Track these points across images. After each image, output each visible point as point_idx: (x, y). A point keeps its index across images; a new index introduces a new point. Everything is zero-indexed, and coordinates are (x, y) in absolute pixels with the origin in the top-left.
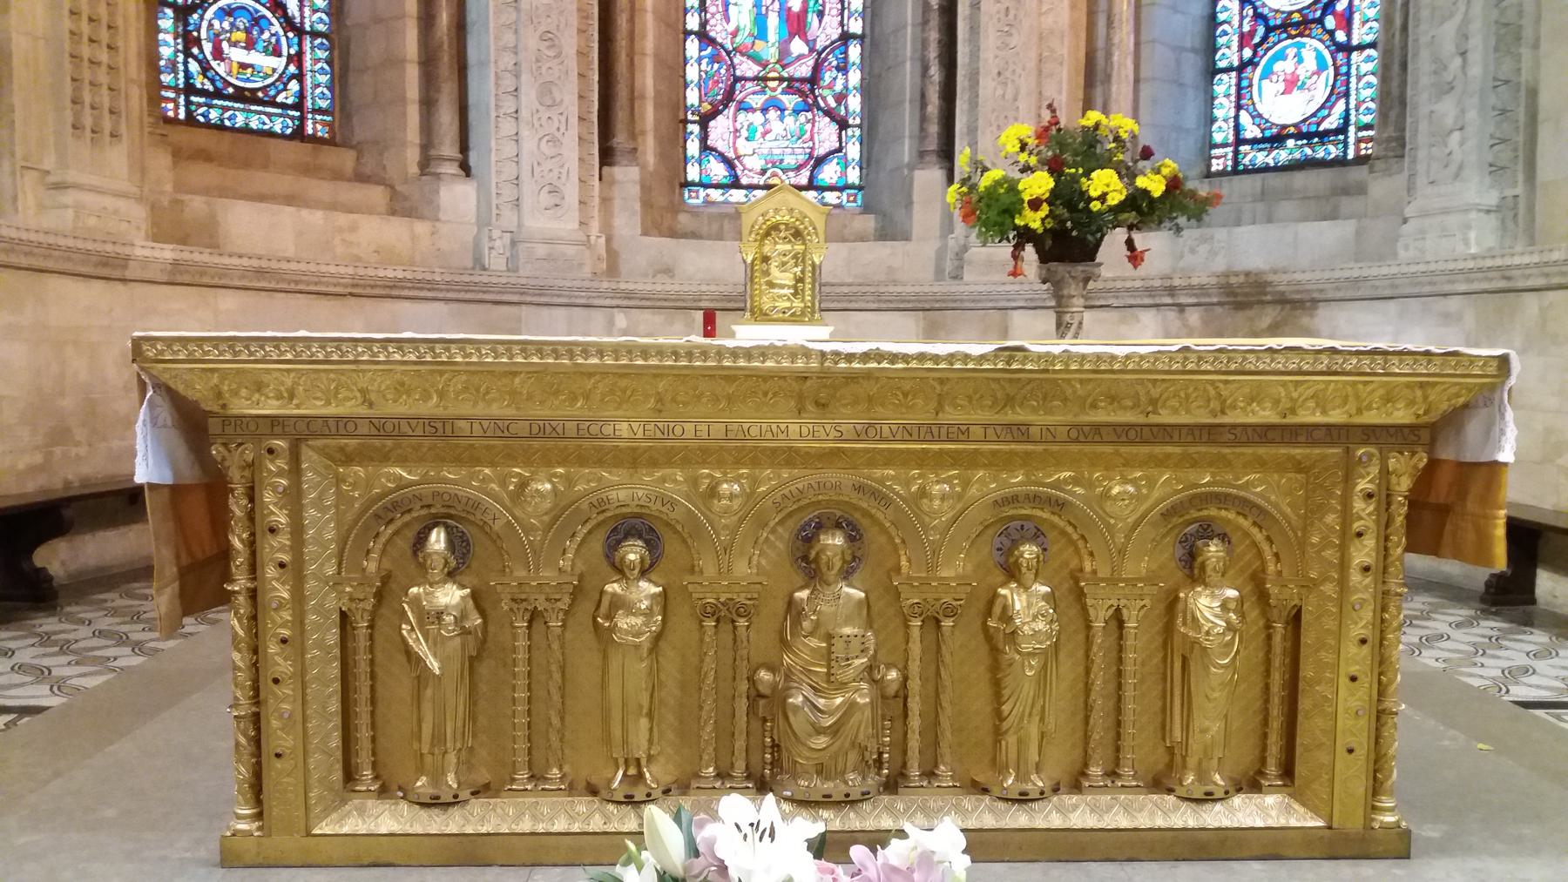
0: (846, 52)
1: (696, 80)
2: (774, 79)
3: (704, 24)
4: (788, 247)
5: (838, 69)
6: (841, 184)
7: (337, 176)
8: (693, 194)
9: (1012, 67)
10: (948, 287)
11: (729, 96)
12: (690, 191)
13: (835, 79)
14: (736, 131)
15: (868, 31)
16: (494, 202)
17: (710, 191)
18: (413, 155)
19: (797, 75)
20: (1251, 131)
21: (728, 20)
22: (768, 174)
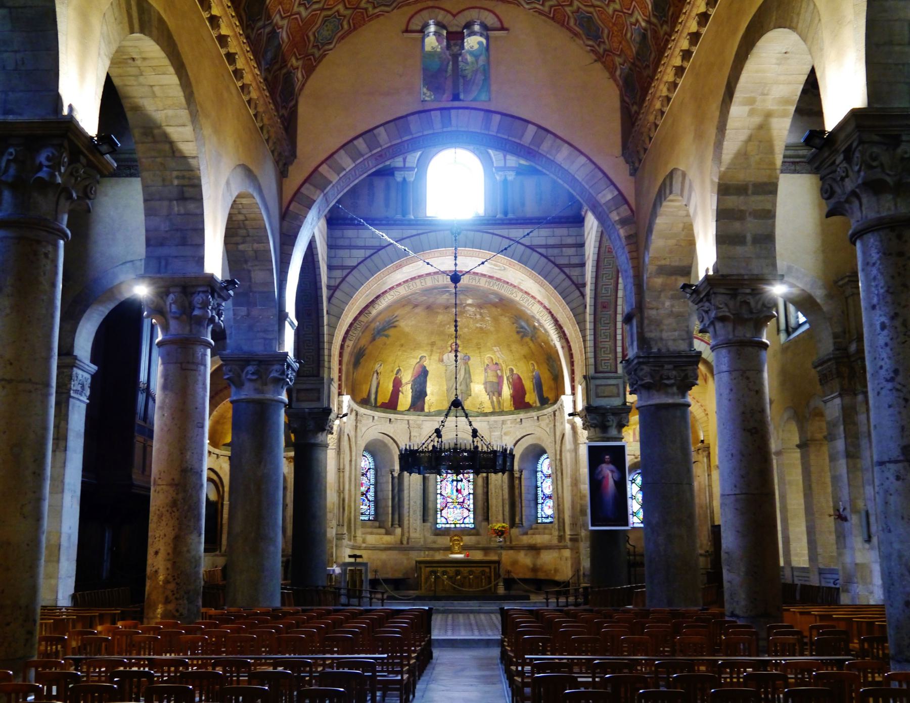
7: (376, 528)
10: (488, 546)
11: (446, 506)
18: (390, 523)
20: (544, 516)
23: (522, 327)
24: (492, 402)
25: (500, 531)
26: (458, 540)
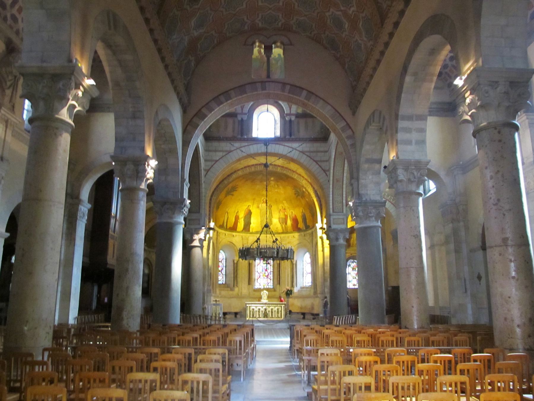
23: (297, 191)
24: (282, 228)
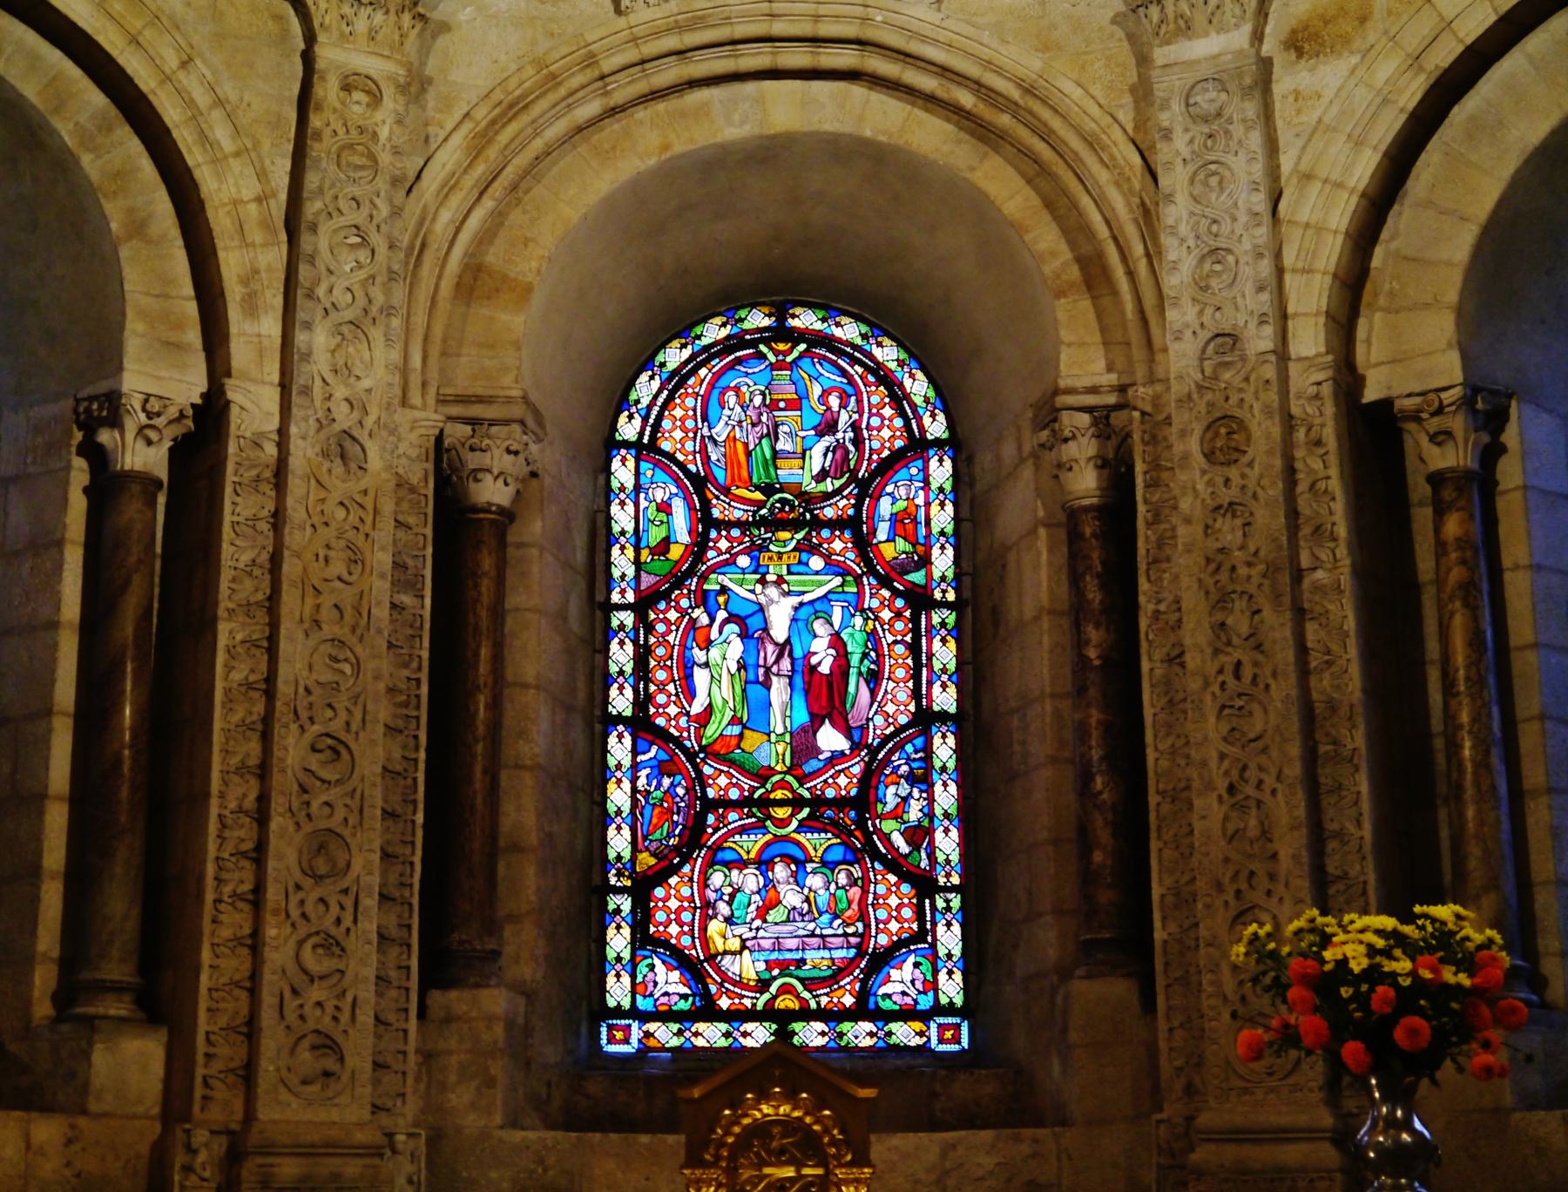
0: (928, 749)
1: (626, 809)
2: (781, 803)
3: (642, 703)
4: (789, 1172)
5: (912, 779)
6: (925, 1002)
8: (619, 1035)
9: (1253, 774)
11: (694, 836)
12: (610, 1028)
13: (905, 800)
14: (707, 904)
15: (968, 707)
16: (200, 1072)
17: (651, 1027)
18: (43, 980)
19: (830, 793)
21: (691, 694)
22: (773, 989)
25: (1412, 996)
26: (805, 1146)
